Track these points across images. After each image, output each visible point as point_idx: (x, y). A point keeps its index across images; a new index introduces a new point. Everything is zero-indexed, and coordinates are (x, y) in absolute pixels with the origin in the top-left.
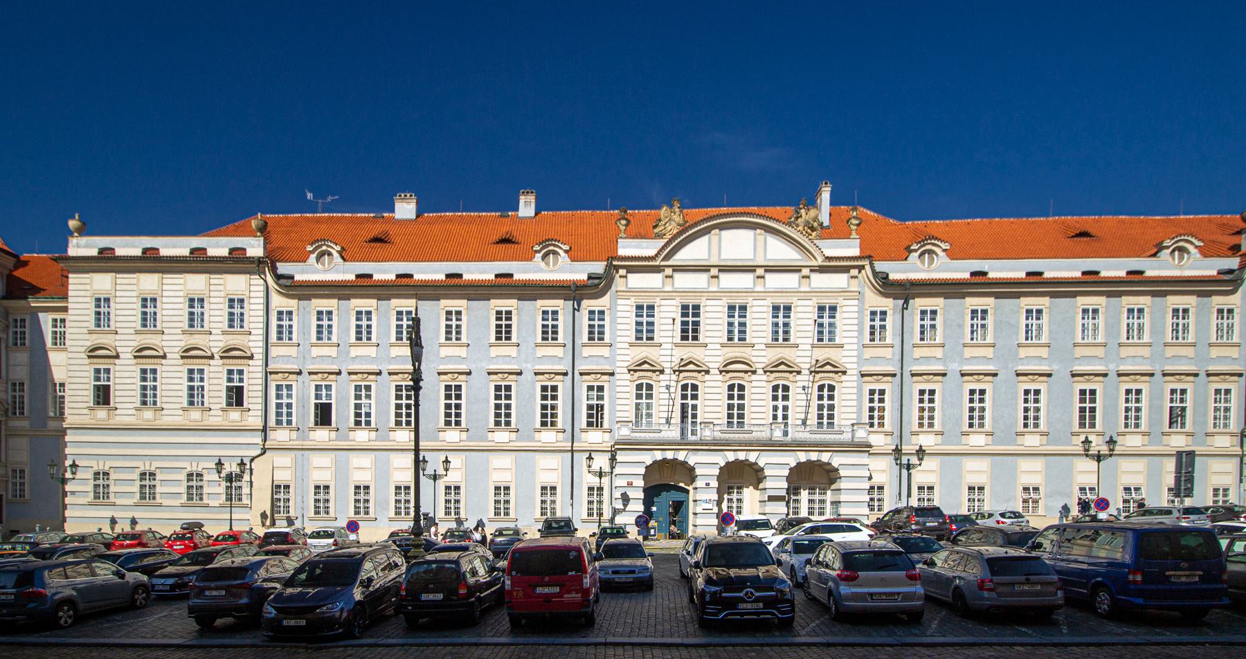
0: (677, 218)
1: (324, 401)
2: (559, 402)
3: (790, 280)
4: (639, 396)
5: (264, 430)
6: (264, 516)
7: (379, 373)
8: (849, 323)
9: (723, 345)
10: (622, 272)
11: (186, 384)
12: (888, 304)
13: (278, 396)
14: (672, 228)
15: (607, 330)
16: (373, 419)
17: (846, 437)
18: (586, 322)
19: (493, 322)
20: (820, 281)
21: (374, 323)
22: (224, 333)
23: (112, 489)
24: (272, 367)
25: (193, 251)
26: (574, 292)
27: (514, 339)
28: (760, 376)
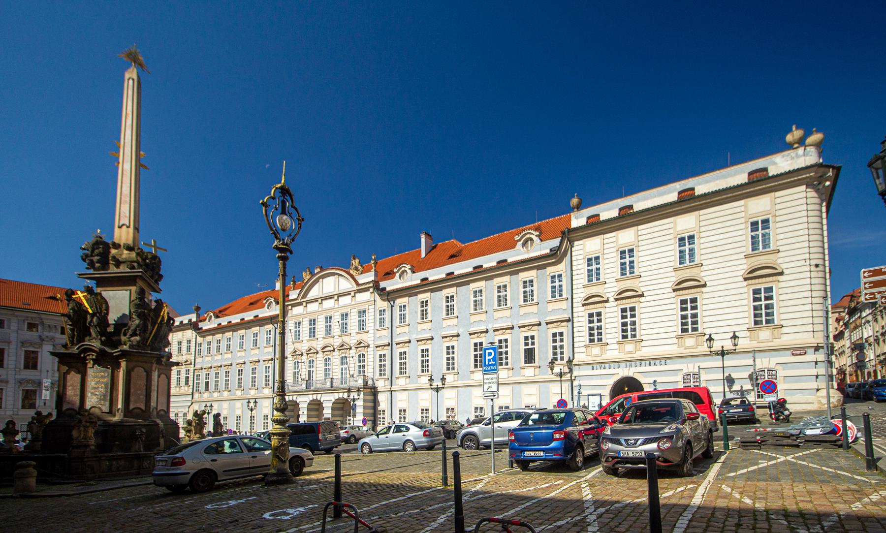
8: (371, 318)
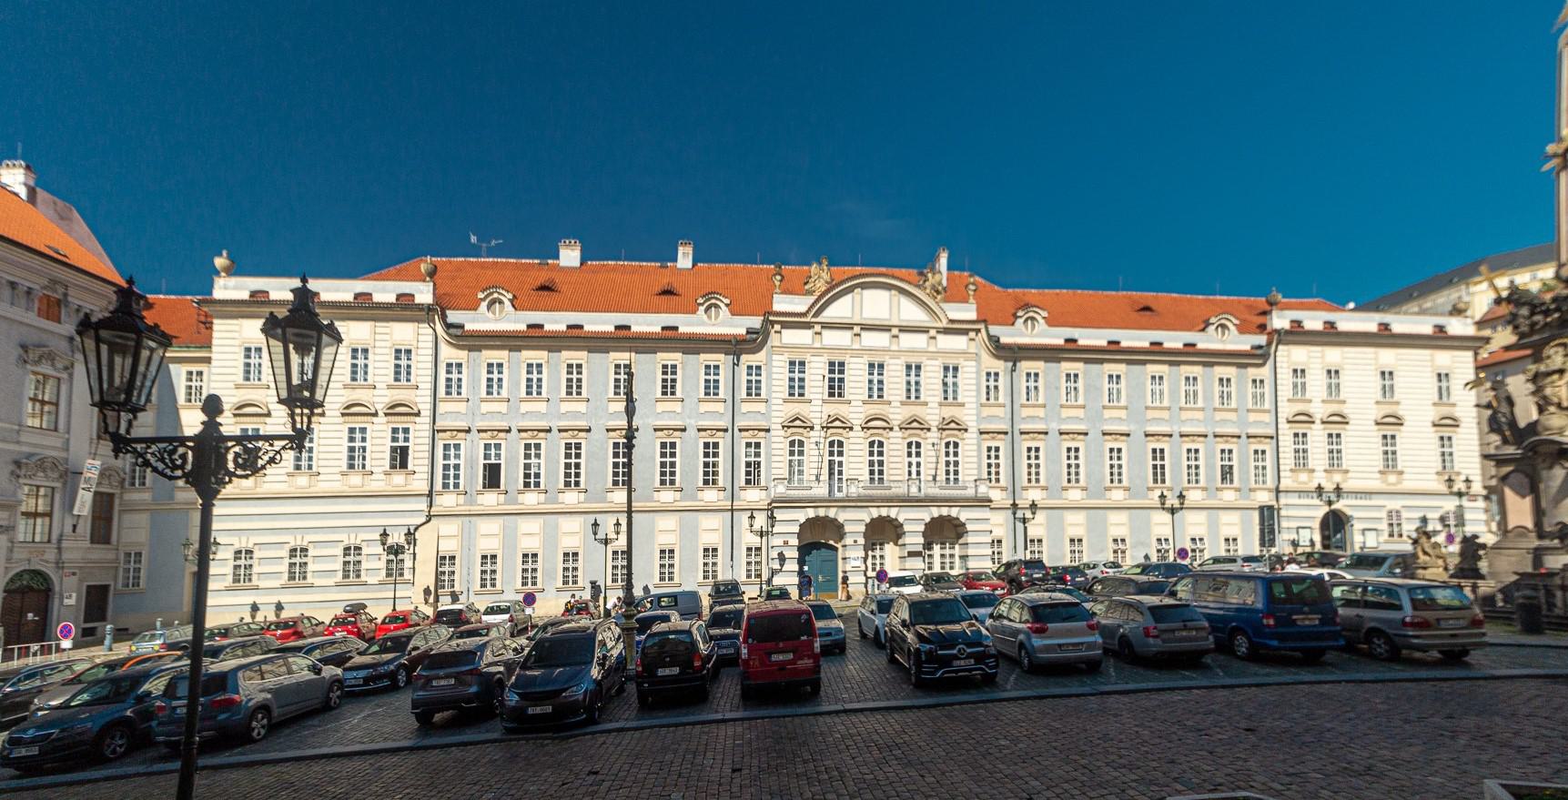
0: (826, 276)
1: (493, 461)
2: (720, 459)
3: (919, 341)
4: (792, 453)
5: (430, 495)
6: (427, 592)
7: (549, 431)
8: (969, 382)
9: (864, 403)
10: (777, 327)
11: (346, 444)
12: (1000, 366)
13: (446, 457)
14: (821, 286)
15: (763, 385)
16: (542, 480)
17: (970, 492)
18: (745, 378)
19: (660, 377)
20: (947, 342)
21: (544, 376)
22: (389, 387)
23: (256, 569)
24: (440, 424)
25: (357, 296)
26: (735, 347)
27: (679, 394)
28: (897, 433)
